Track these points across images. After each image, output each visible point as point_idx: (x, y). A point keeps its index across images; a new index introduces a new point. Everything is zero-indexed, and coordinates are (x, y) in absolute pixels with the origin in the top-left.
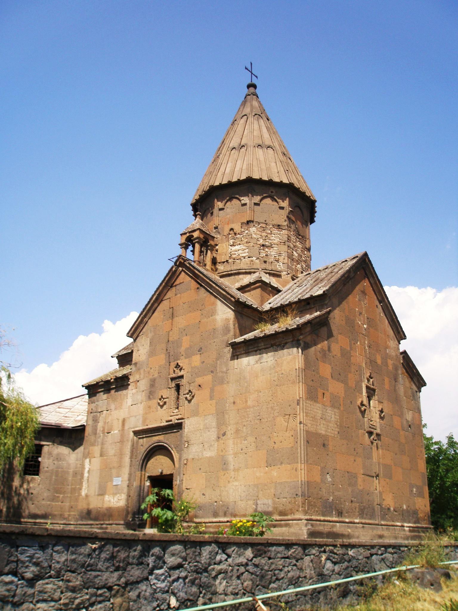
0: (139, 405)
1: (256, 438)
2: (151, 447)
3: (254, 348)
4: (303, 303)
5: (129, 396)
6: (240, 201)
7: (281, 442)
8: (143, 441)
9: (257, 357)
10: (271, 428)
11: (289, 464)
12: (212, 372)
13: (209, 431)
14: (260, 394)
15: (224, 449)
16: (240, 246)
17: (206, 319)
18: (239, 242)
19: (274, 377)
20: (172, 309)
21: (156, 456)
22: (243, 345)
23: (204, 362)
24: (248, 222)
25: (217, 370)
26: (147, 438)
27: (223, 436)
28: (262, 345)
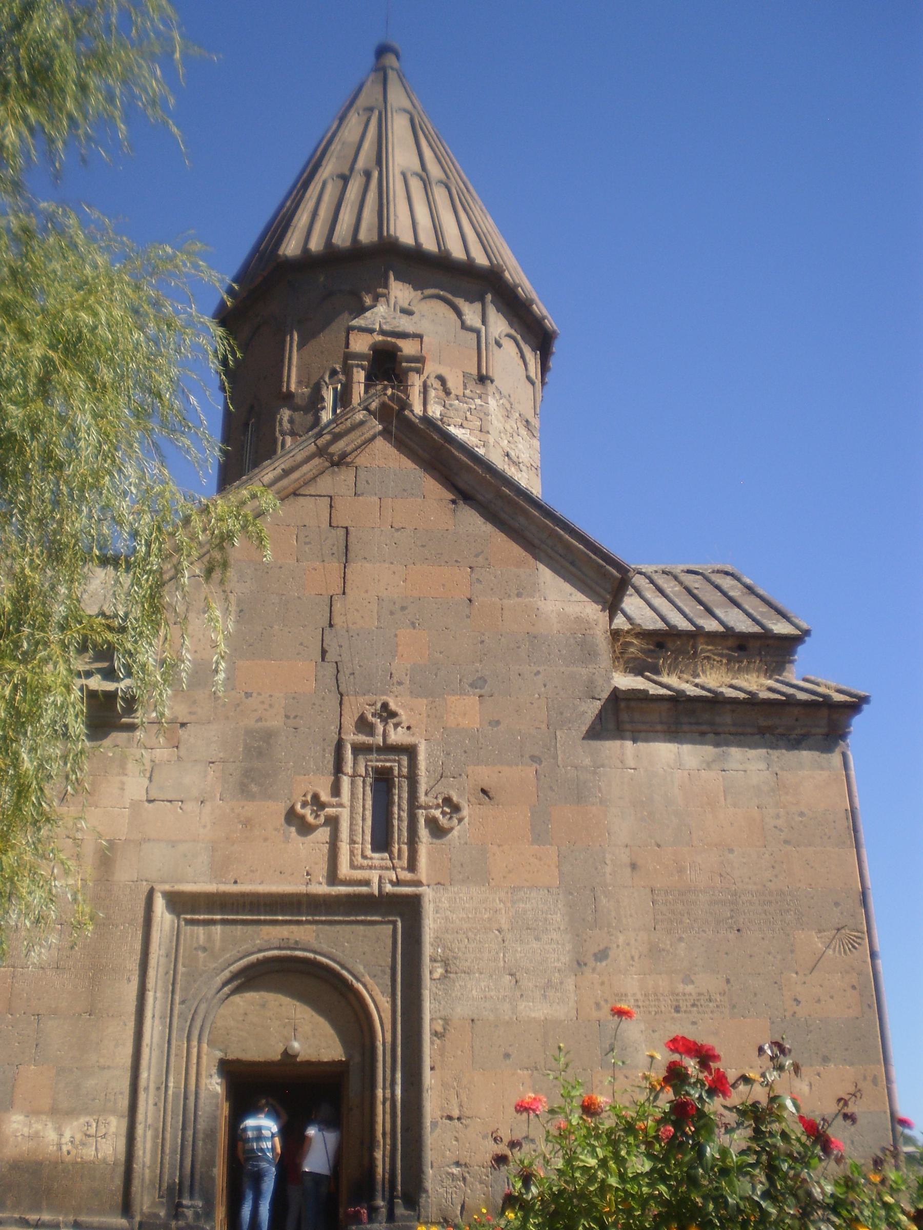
0: (190, 806)
1: (728, 981)
2: (253, 958)
3: (697, 724)
4: (730, 643)
5: (131, 766)
6: (459, 313)
7: (819, 1001)
8: (209, 938)
9: (708, 751)
10: (779, 957)
11: (851, 1064)
12: (534, 759)
13: (537, 939)
14: (731, 856)
15: (606, 1001)
16: (463, 431)
17: (495, 599)
18: (459, 421)
19: (778, 816)
20: (342, 532)
21: (269, 989)
22: (665, 706)
23: (498, 723)
24: (483, 379)
25: (555, 757)
26: (228, 928)
27: (601, 960)
28: (727, 719)
